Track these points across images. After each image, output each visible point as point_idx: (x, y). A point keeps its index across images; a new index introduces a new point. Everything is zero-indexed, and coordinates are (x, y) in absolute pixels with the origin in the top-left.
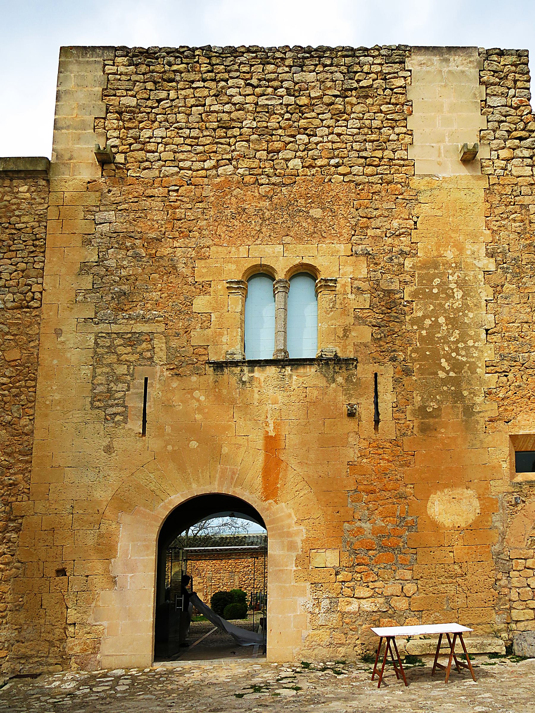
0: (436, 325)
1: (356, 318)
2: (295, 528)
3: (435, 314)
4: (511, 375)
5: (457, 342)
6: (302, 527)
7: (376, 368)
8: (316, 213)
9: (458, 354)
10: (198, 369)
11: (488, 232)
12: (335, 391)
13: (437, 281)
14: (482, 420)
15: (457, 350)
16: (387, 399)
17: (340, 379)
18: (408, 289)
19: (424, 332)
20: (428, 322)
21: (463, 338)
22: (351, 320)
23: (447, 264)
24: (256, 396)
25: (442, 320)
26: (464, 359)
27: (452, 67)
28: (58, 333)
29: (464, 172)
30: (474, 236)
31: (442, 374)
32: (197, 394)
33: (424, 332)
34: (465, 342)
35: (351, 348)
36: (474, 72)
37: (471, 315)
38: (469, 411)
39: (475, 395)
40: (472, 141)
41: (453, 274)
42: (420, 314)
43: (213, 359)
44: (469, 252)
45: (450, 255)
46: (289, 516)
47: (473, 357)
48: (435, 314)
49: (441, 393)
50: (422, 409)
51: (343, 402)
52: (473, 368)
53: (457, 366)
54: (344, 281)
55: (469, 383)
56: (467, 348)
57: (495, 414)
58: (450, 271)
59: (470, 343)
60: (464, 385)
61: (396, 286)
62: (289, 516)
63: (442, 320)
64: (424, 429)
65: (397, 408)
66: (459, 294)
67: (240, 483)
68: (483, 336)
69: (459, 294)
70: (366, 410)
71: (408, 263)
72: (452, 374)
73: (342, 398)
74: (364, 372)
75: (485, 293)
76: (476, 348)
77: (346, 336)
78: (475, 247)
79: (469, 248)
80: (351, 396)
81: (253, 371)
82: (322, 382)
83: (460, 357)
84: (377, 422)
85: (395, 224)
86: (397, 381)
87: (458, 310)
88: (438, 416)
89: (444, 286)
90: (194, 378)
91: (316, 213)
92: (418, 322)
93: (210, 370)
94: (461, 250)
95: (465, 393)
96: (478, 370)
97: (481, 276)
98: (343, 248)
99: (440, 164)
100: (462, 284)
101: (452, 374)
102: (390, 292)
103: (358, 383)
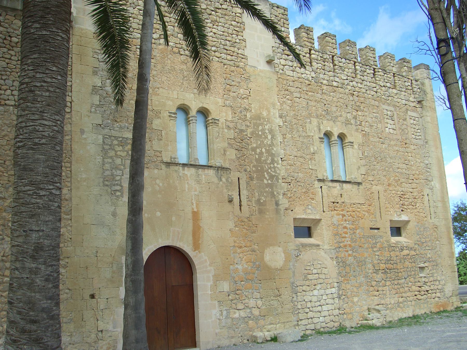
0: (261, 153)
1: (229, 143)
2: (209, 268)
4: (292, 185)
5: (270, 164)
6: (212, 268)
7: (238, 174)
9: (271, 171)
10: (157, 165)
11: (279, 104)
12: (222, 186)
13: (260, 128)
15: (270, 168)
16: (244, 193)
17: (224, 180)
18: (250, 130)
19: (257, 156)
20: (258, 151)
22: (226, 145)
23: (263, 118)
24: (187, 186)
25: (264, 150)
26: (274, 174)
28: (82, 132)
29: (266, 68)
31: (265, 181)
32: (158, 181)
33: (257, 156)
34: (274, 164)
35: (227, 162)
37: (275, 149)
39: (279, 195)
41: (266, 125)
42: (255, 145)
43: (165, 160)
44: (272, 114)
45: (265, 113)
46: (206, 261)
47: (277, 173)
49: (266, 192)
50: (259, 200)
52: (277, 179)
53: (272, 177)
54: (222, 120)
55: (276, 188)
56: (274, 168)
57: (287, 206)
58: (265, 123)
59: (276, 165)
60: (274, 188)
61: (244, 128)
62: (206, 261)
63: (264, 150)
64: (261, 212)
66: (269, 137)
67: (197, 246)
68: (280, 162)
69: (269, 137)
71: (248, 115)
72: (269, 182)
73: (225, 190)
74: (234, 176)
75: (279, 138)
76: (278, 168)
77: (225, 154)
78: (275, 111)
80: (229, 190)
81: (184, 170)
82: (215, 180)
83: (272, 172)
84: (240, 206)
85: (242, 91)
86: (248, 183)
87: (270, 146)
88: (265, 205)
90: (156, 171)
92: (254, 149)
93: (163, 167)
94: (269, 111)
95: (275, 193)
96: (280, 180)
97: (277, 128)
99: (258, 61)
100: (271, 131)
101: (269, 182)
102: (242, 131)
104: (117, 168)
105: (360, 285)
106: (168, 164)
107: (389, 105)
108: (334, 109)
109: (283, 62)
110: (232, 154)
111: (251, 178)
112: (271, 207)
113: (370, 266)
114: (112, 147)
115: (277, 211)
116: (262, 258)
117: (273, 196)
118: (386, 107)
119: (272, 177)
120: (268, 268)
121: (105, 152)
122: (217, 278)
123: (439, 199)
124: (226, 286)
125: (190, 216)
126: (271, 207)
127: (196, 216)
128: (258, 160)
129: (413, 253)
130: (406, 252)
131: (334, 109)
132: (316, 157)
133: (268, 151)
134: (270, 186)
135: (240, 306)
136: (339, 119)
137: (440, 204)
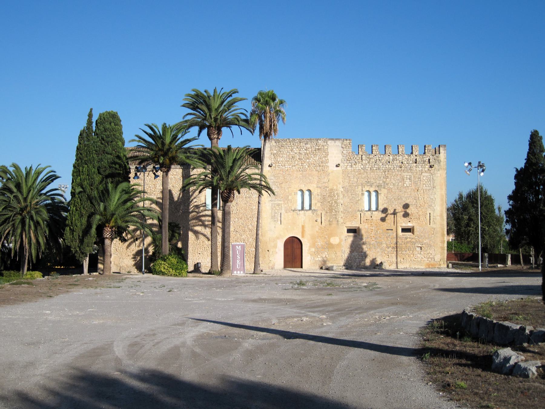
3: (332, 200)
8: (310, 178)
14: (340, 223)
21: (337, 206)
22: (317, 202)
27: (336, 144)
30: (340, 183)
36: (340, 145)
38: (338, 221)
40: (339, 162)
45: (335, 188)
48: (332, 200)
51: (315, 219)
52: (339, 212)
53: (336, 211)
64: (330, 224)
65: (325, 220)
70: (319, 220)
75: (341, 196)
79: (339, 186)
82: (312, 214)
89: (334, 194)
91: (310, 178)
92: (329, 202)
98: (315, 186)
100: (337, 194)
103: (318, 215)
104: (276, 213)
105: (378, 252)
106: (294, 211)
107: (408, 172)
108: (372, 180)
109: (346, 164)
110: (319, 204)
111: (327, 212)
112: (335, 222)
113: (385, 245)
114: (274, 207)
115: (338, 224)
116: (329, 241)
117: (336, 218)
118: (406, 174)
119: (336, 211)
120: (332, 244)
121: (272, 209)
122: (310, 247)
123: (438, 215)
124: (313, 250)
125: (301, 227)
126: (335, 222)
127: (303, 227)
128: (331, 206)
129: (414, 240)
130: (408, 240)
131: (372, 180)
132: (359, 202)
133: (335, 202)
134: (335, 215)
135: (319, 256)
136: (375, 184)
137: (438, 218)
